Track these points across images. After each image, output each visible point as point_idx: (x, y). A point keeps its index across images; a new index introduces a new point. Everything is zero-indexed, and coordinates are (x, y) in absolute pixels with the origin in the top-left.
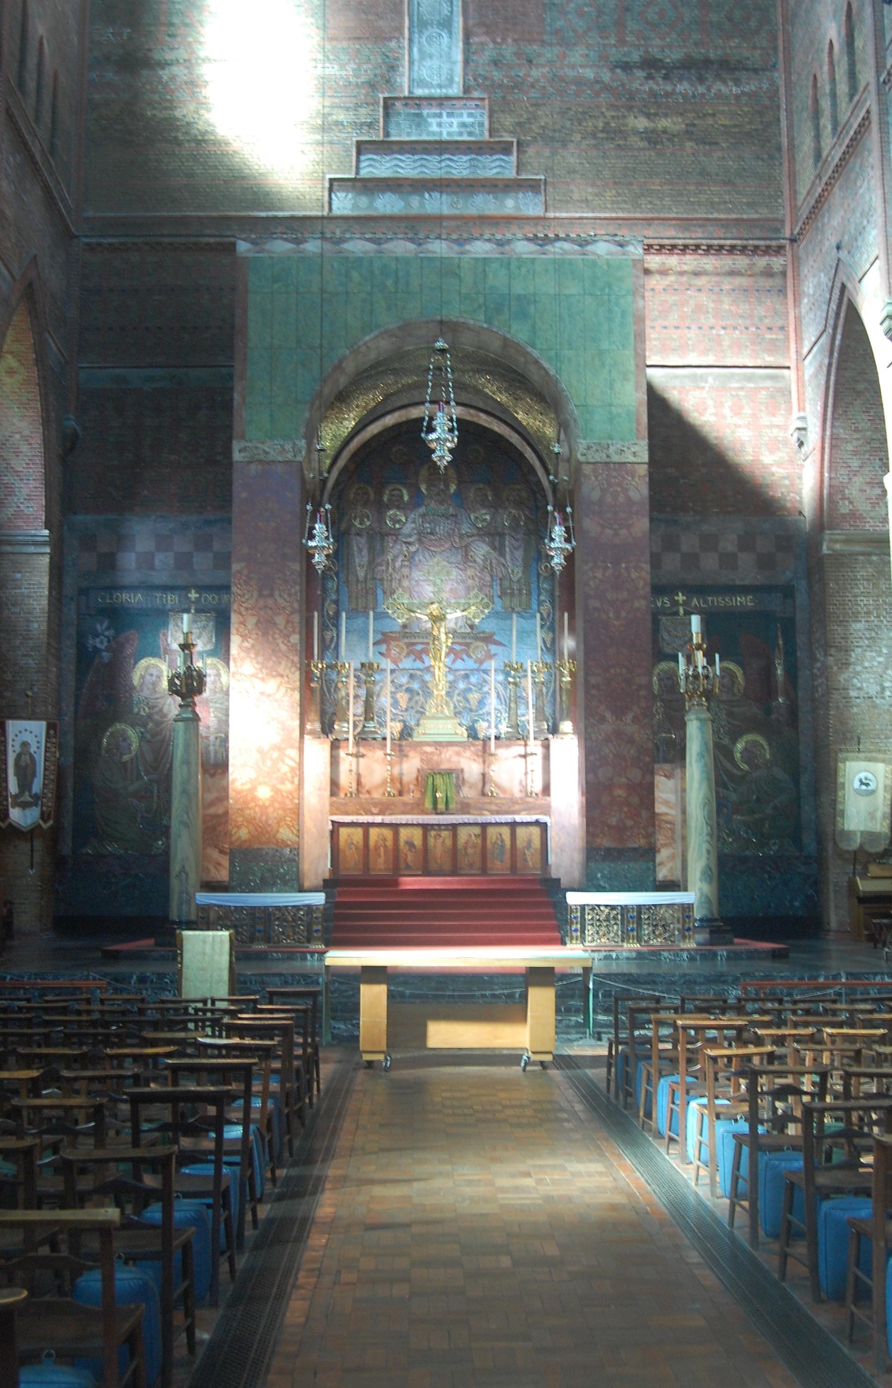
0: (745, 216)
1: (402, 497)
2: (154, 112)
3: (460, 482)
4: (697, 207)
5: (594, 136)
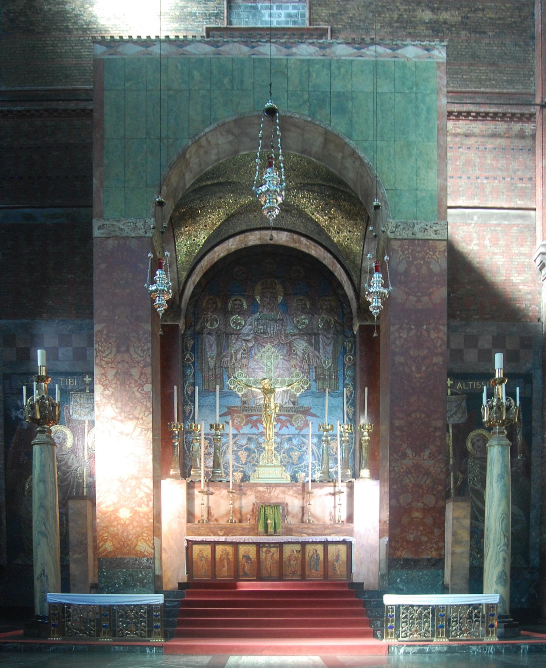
0: (505, 91)
1: (242, 305)
2: (49, 7)
3: (285, 295)
4: (468, 83)
5: (390, 25)
